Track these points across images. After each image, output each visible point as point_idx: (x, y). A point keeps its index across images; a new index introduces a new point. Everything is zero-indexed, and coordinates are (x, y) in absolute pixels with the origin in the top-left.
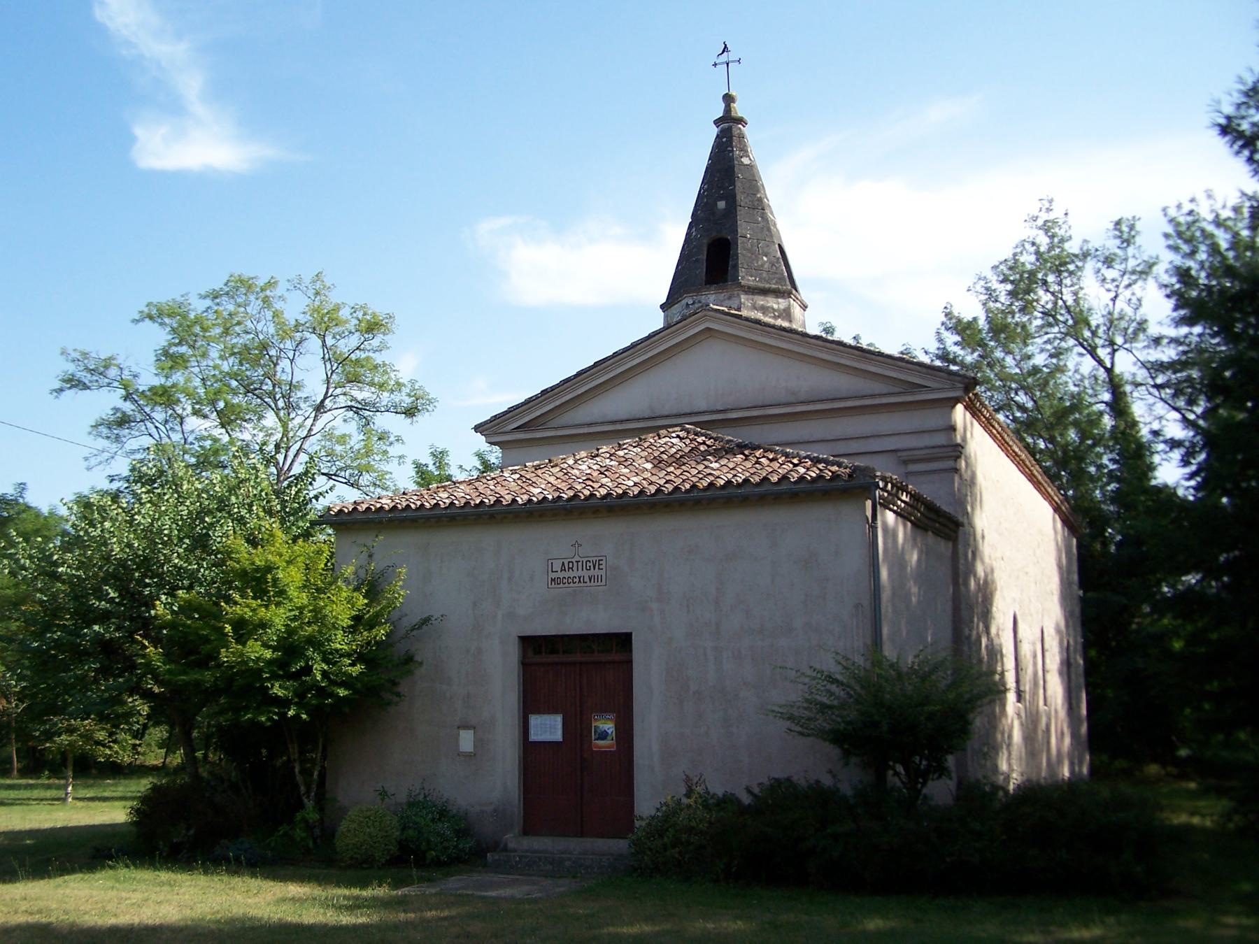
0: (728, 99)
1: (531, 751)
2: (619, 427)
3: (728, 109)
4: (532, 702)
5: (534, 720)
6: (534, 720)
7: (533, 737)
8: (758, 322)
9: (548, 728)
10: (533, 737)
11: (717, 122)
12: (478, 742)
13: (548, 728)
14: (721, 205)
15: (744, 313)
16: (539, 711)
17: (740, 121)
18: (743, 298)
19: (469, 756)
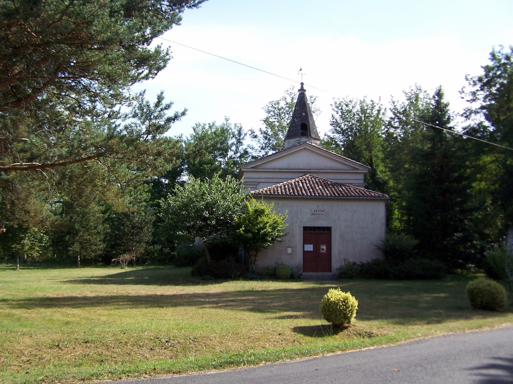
0: (302, 84)
1: (305, 253)
2: (281, 170)
3: (302, 87)
4: (306, 241)
5: (305, 246)
6: (305, 246)
7: (305, 250)
8: (315, 146)
9: (309, 248)
10: (305, 250)
11: (299, 90)
12: (292, 251)
13: (309, 248)
14: (304, 114)
15: (313, 145)
16: (307, 244)
17: (305, 91)
18: (312, 140)
19: (290, 254)
